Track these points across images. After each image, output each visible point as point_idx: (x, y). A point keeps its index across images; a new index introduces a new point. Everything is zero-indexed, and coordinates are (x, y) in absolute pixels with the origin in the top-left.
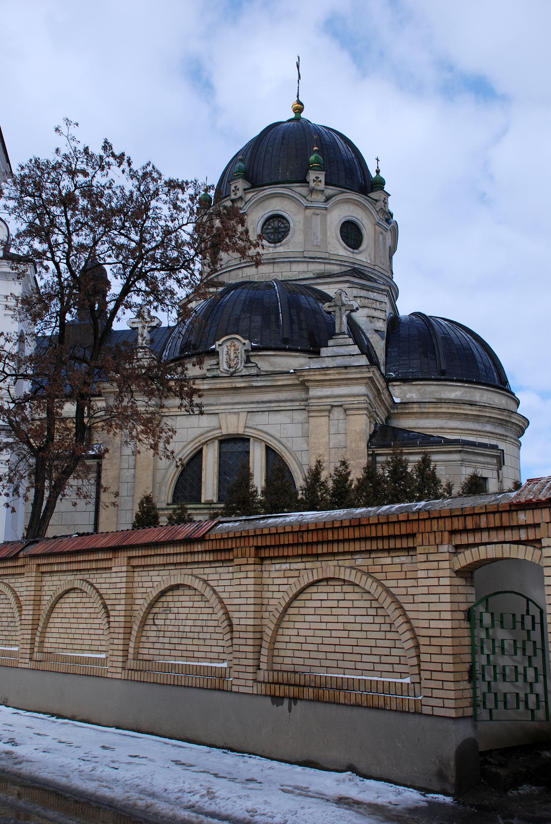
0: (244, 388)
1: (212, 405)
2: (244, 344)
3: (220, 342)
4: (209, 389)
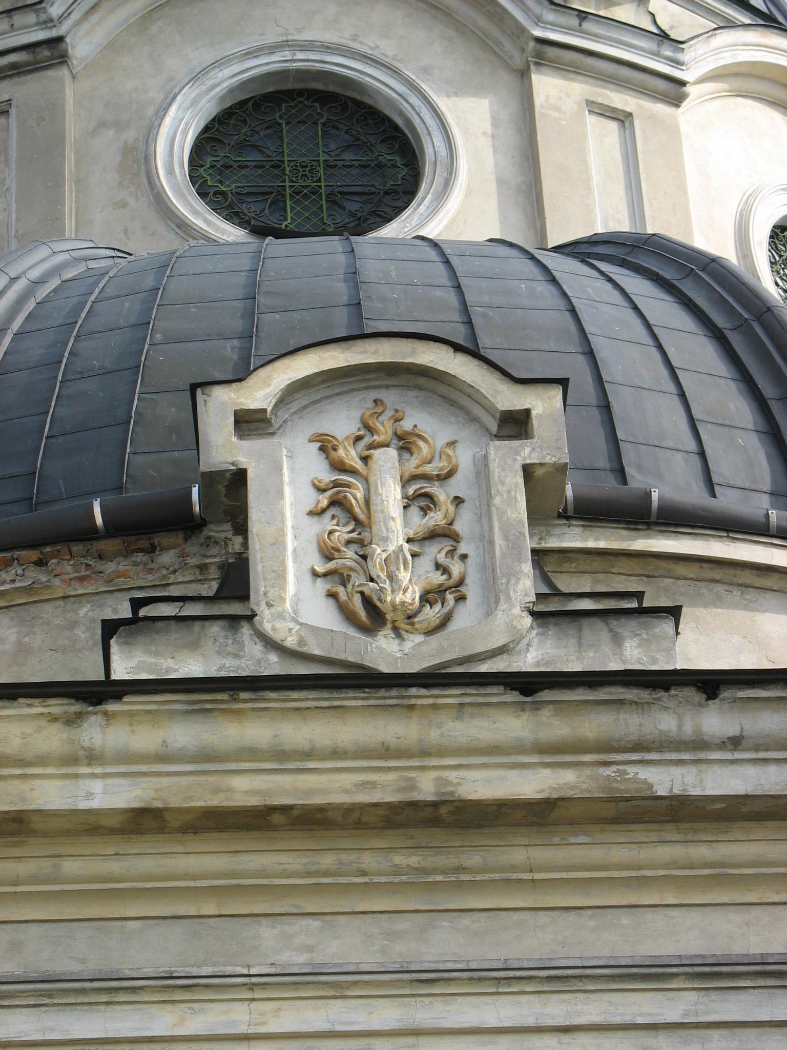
0: (539, 815)
1: (175, 986)
2: (516, 424)
3: (262, 391)
4: (144, 822)
